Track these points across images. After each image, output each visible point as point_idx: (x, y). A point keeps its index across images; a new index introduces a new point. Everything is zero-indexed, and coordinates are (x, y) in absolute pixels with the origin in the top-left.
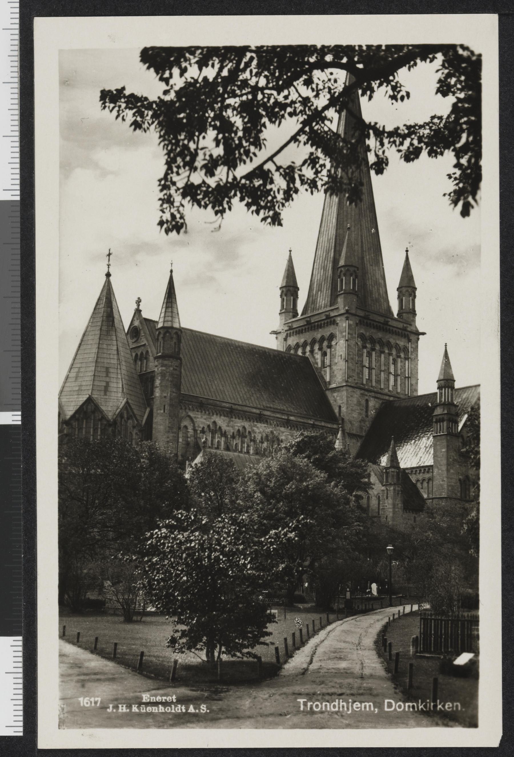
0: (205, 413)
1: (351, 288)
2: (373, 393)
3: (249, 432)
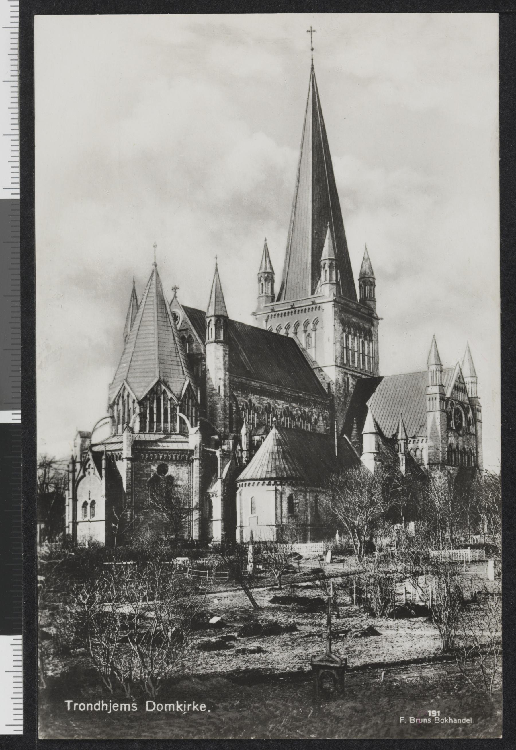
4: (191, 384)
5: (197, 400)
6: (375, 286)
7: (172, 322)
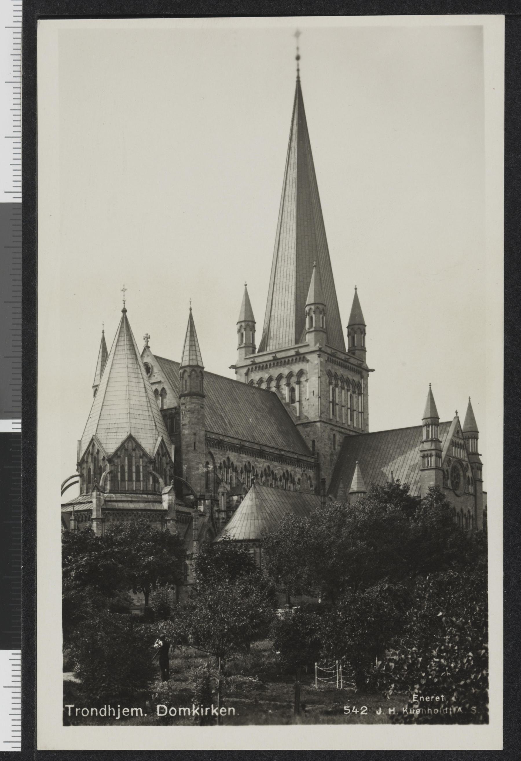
0: (222, 449)
1: (321, 326)
2: (339, 428)
3: (253, 467)
4: (165, 440)
5: (170, 458)
6: (365, 334)
7: (144, 373)
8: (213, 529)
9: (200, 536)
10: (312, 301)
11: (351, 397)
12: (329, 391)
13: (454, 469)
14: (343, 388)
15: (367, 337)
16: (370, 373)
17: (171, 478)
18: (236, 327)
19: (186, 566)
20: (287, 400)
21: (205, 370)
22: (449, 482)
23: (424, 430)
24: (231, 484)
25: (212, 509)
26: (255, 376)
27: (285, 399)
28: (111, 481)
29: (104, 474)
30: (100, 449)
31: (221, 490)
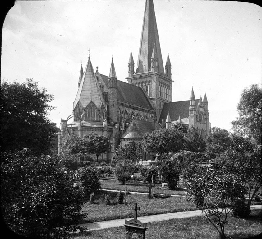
4: (104, 103)
5: (105, 109)
6: (171, 69)
7: (96, 80)
8: (120, 134)
9: (116, 136)
10: (154, 57)
11: (166, 90)
12: (159, 88)
13: (200, 115)
14: (164, 87)
15: (172, 70)
16: (173, 82)
17: (106, 116)
18: (128, 65)
19: (111, 147)
20: (145, 91)
21: (117, 79)
22: (198, 119)
23: (190, 102)
24: (126, 118)
25: (120, 127)
26: (134, 82)
27: (144, 90)
28: (85, 117)
29: (82, 114)
30: (81, 106)
31: (123, 121)
